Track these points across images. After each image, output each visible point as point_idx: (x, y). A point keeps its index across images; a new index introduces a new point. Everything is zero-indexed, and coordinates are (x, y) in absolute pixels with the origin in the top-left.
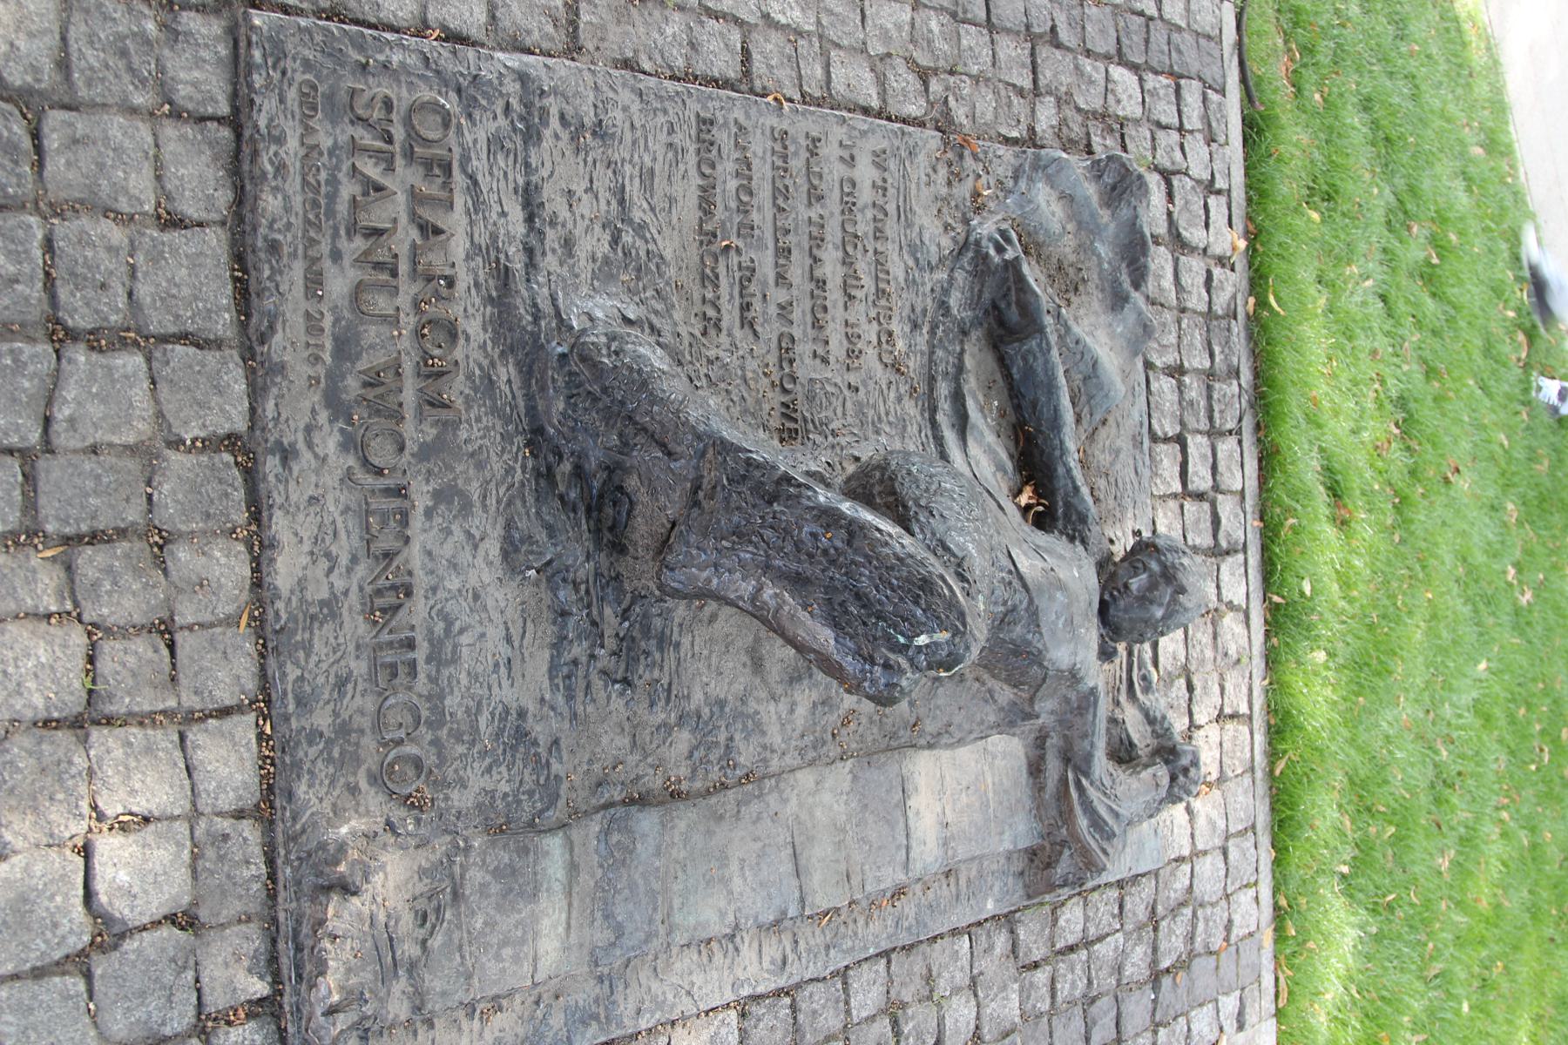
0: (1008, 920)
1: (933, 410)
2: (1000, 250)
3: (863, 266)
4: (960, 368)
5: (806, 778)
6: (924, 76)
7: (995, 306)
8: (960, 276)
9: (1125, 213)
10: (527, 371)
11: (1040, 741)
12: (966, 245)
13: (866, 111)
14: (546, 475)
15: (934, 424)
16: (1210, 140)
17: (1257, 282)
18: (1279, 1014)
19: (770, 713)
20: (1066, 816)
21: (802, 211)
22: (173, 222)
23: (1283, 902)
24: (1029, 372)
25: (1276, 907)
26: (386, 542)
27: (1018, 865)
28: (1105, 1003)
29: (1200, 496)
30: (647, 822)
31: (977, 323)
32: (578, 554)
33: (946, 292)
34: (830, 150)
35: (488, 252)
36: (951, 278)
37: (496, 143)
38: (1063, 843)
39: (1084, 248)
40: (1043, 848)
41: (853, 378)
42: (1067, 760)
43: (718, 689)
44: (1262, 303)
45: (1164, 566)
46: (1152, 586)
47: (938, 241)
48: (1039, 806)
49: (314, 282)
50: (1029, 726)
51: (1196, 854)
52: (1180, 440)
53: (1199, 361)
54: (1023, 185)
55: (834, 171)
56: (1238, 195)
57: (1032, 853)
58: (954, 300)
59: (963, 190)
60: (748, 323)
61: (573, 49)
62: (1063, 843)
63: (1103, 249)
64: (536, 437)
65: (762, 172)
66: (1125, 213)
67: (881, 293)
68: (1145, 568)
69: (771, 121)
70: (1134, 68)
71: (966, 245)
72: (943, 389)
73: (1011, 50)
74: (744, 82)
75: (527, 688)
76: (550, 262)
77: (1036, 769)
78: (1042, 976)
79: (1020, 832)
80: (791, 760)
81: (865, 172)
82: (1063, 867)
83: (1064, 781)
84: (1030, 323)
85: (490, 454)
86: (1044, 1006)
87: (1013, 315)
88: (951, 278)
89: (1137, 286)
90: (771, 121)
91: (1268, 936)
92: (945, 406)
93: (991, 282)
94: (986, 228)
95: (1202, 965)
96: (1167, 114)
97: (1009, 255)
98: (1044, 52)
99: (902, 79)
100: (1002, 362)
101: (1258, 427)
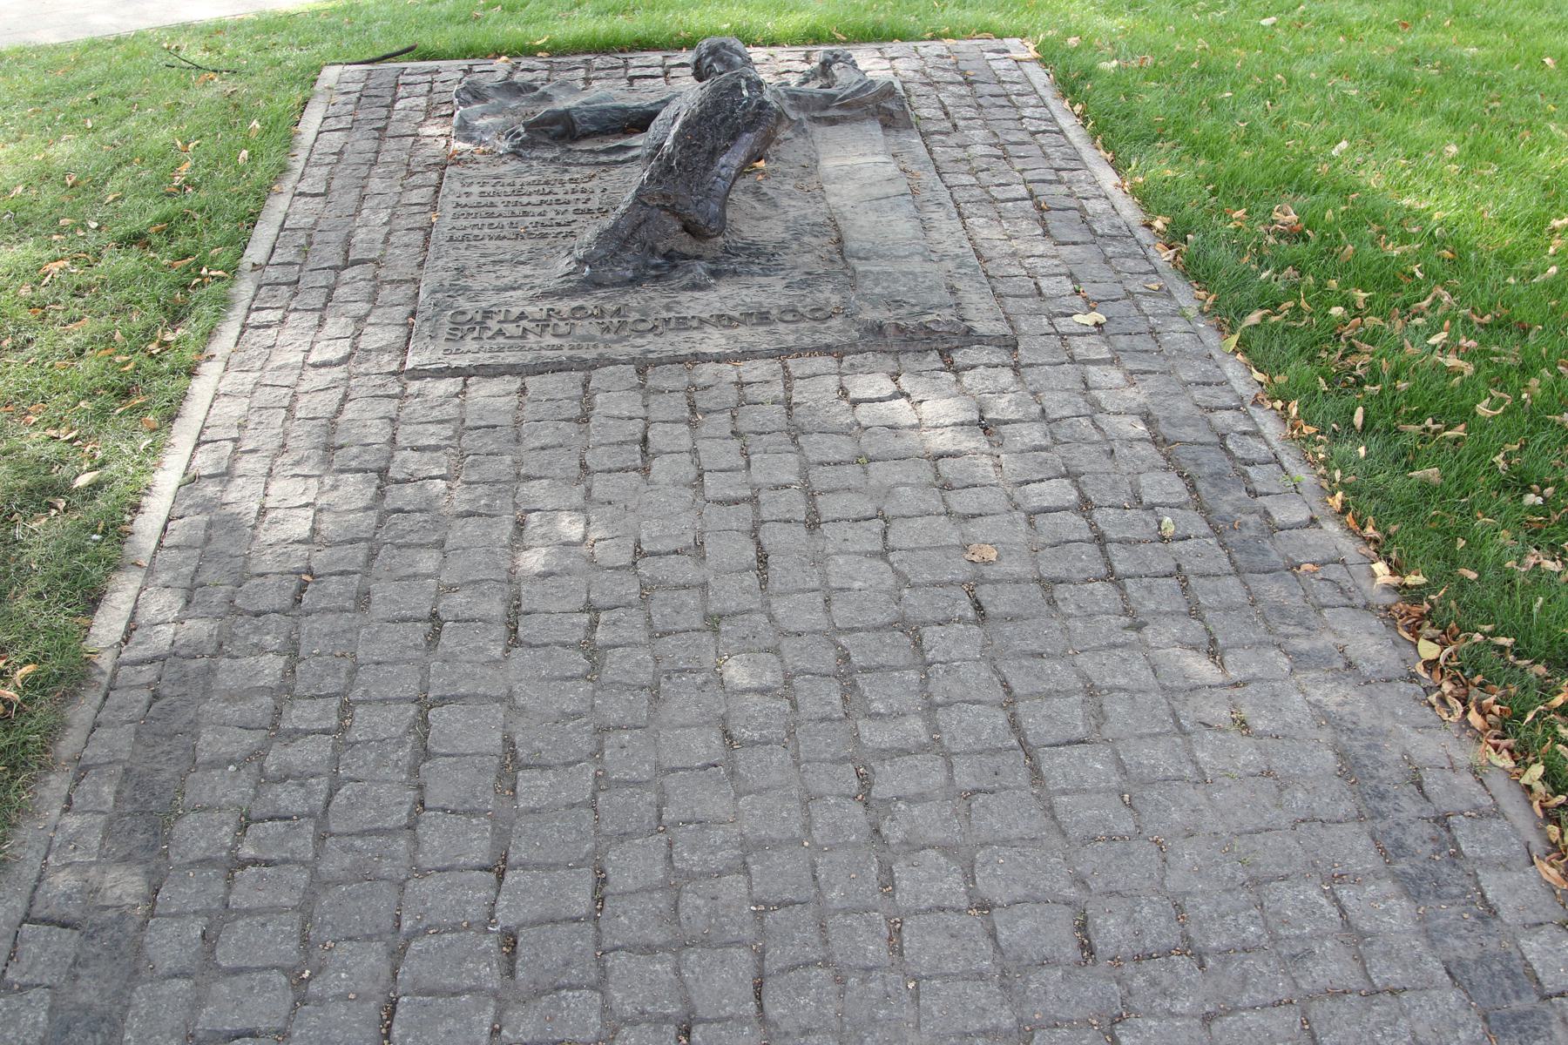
0: (924, 135)
1: (617, 162)
2: (519, 135)
3: (532, 189)
4: (591, 151)
5: (832, 200)
6: (411, 174)
7: (553, 138)
8: (534, 154)
9: (490, 92)
10: (600, 285)
11: (815, 120)
12: (515, 154)
13: (437, 192)
14: (657, 278)
15: (624, 162)
16: (437, 72)
17: (530, 52)
18: (1001, 38)
19: (792, 213)
20: (861, 104)
21: (501, 208)
22: (523, 390)
23: (929, 35)
24: (593, 120)
25: (932, 39)
26: (695, 323)
27: (893, 132)
28: (981, 101)
29: (667, 73)
30: (851, 245)
31: (562, 146)
32: (700, 268)
33: (545, 160)
34: (463, 200)
35: (533, 300)
36: (537, 158)
37: (469, 299)
38: (878, 107)
39: (514, 112)
40: (881, 121)
41: (598, 191)
42: (826, 108)
43: (780, 229)
44: (541, 48)
45: (708, 54)
46: (721, 60)
47: (515, 164)
48: (855, 119)
49: (553, 348)
50: (806, 126)
51: (892, 68)
52: (631, 79)
53: (582, 73)
54: (476, 134)
55: (474, 199)
56: (471, 62)
57: (885, 126)
58: (549, 155)
59: (481, 158)
60: (569, 224)
61: (415, 281)
62: (878, 107)
63: (514, 104)
64: (636, 281)
65: (478, 221)
66: (490, 92)
67: (547, 183)
68: (710, 66)
69: (448, 219)
70: (394, 102)
71: (515, 154)
72: (603, 158)
73: (391, 144)
74: (427, 231)
75: (777, 283)
76: (537, 282)
77: (833, 121)
78: (961, 123)
79: (873, 129)
80: (823, 205)
81: (475, 189)
82: (891, 106)
83: (839, 107)
84: (565, 117)
85: (648, 299)
86: (980, 122)
87: (558, 128)
88: (537, 158)
89: (536, 89)
90: (448, 219)
91: (950, 42)
92: (613, 158)
93: (538, 138)
94: (505, 145)
95: (962, 65)
96: (426, 87)
97: (522, 130)
98: (390, 132)
99: (417, 180)
100: (586, 136)
101: (622, 51)
